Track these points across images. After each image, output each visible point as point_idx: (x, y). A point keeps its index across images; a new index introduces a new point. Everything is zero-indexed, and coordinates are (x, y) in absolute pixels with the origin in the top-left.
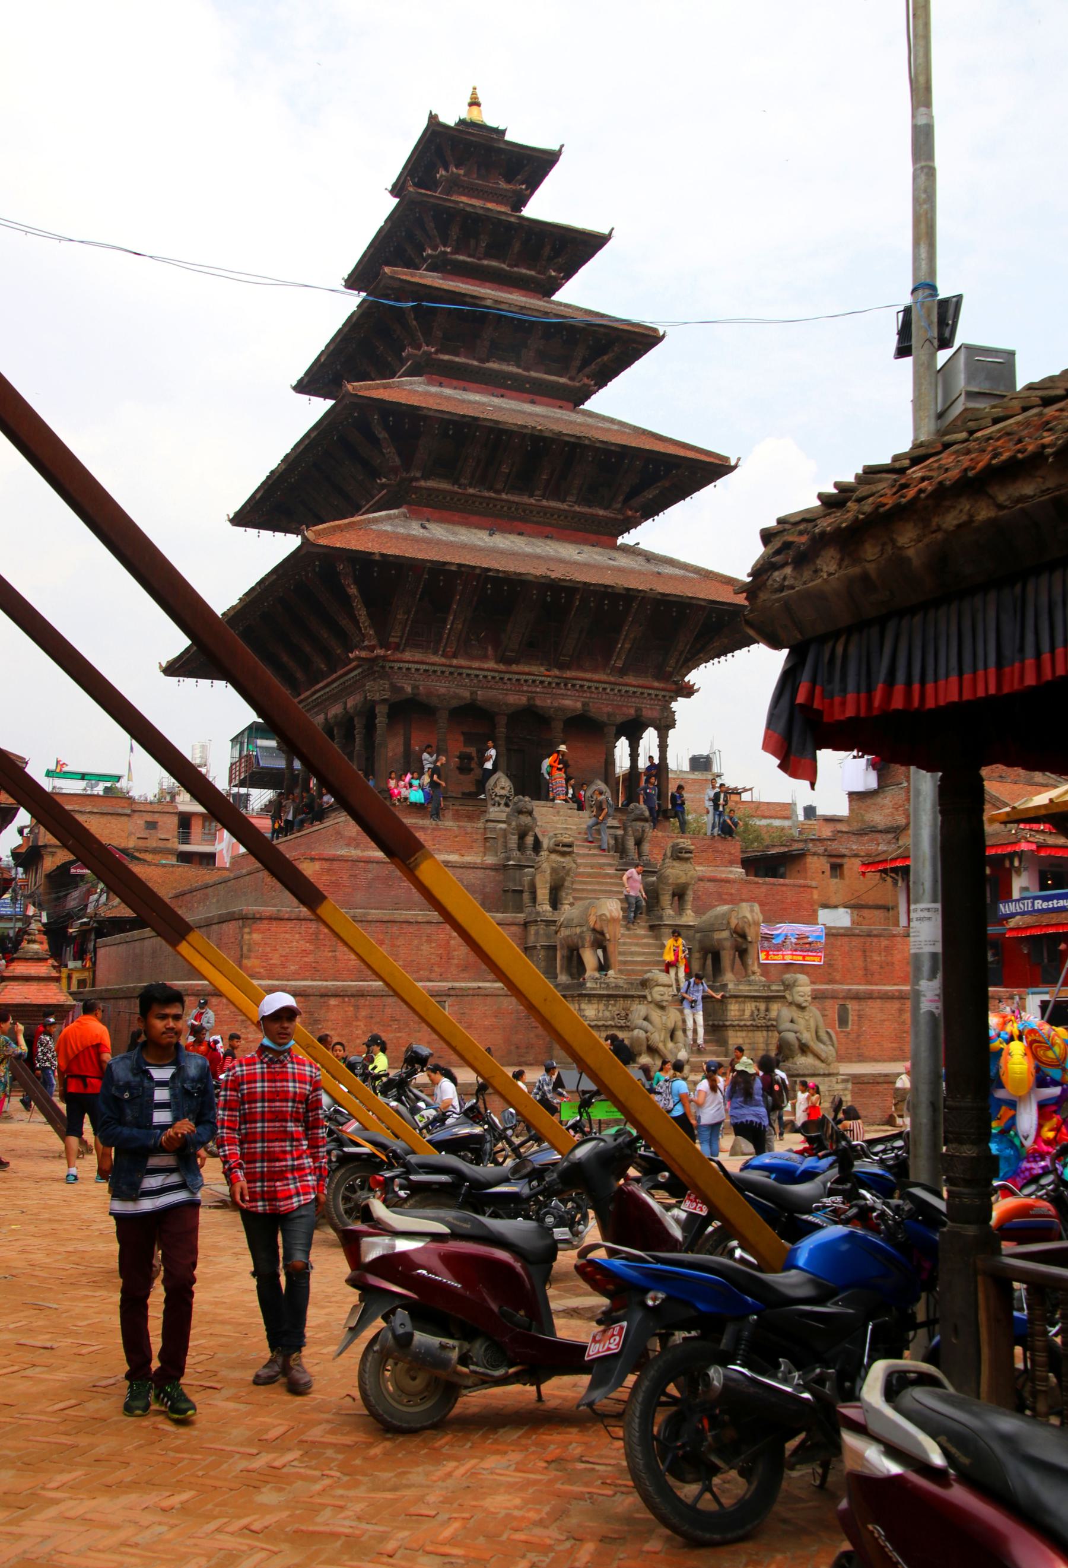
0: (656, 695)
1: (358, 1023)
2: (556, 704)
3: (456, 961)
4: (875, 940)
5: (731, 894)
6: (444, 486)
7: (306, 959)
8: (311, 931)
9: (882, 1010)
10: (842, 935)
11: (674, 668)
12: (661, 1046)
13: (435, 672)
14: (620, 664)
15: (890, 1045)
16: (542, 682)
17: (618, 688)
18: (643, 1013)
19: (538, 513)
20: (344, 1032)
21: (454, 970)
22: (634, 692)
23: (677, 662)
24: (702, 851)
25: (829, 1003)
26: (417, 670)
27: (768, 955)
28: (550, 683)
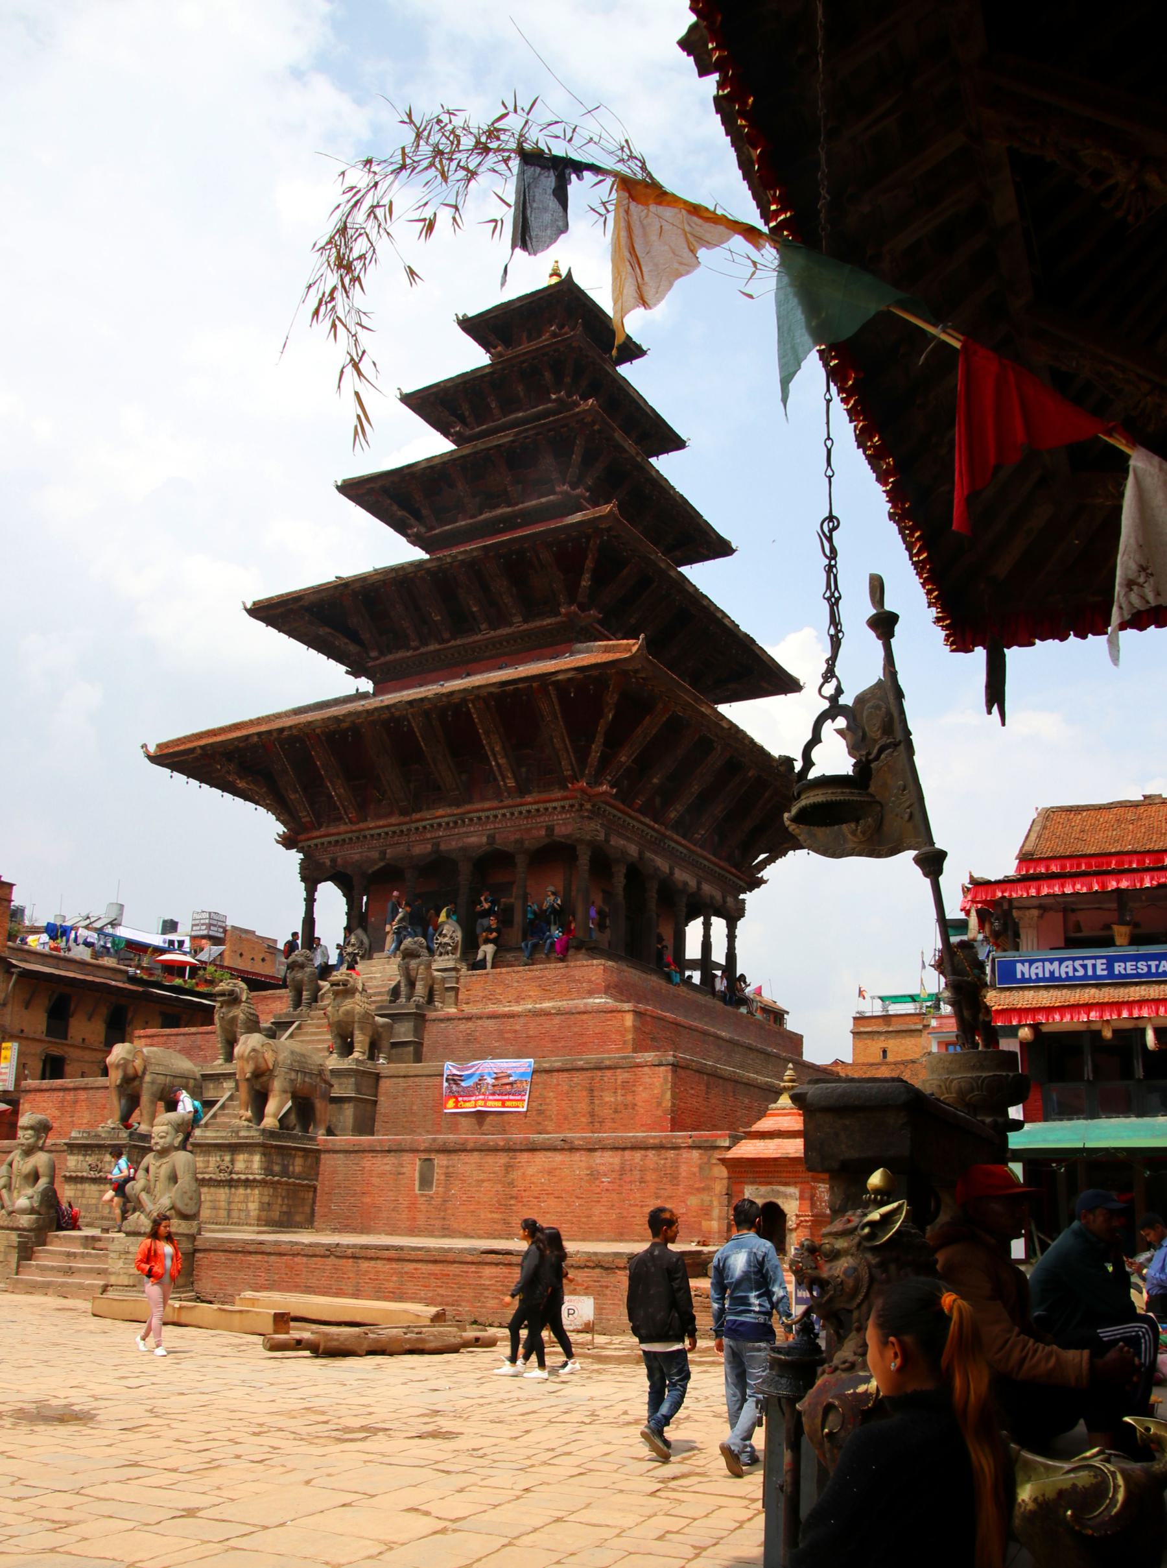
0: (563, 807)
2: (460, 845)
4: (608, 1073)
5: (516, 1031)
6: (401, 654)
9: (480, 1166)
10: (558, 1071)
11: (573, 769)
13: (344, 840)
14: (511, 783)
15: (489, 1216)
16: (440, 825)
17: (516, 811)
18: (10, 1158)
19: (487, 647)
22: (538, 810)
23: (572, 764)
24: (555, 983)
25: (407, 1157)
26: (330, 842)
27: (457, 1102)
28: (448, 824)
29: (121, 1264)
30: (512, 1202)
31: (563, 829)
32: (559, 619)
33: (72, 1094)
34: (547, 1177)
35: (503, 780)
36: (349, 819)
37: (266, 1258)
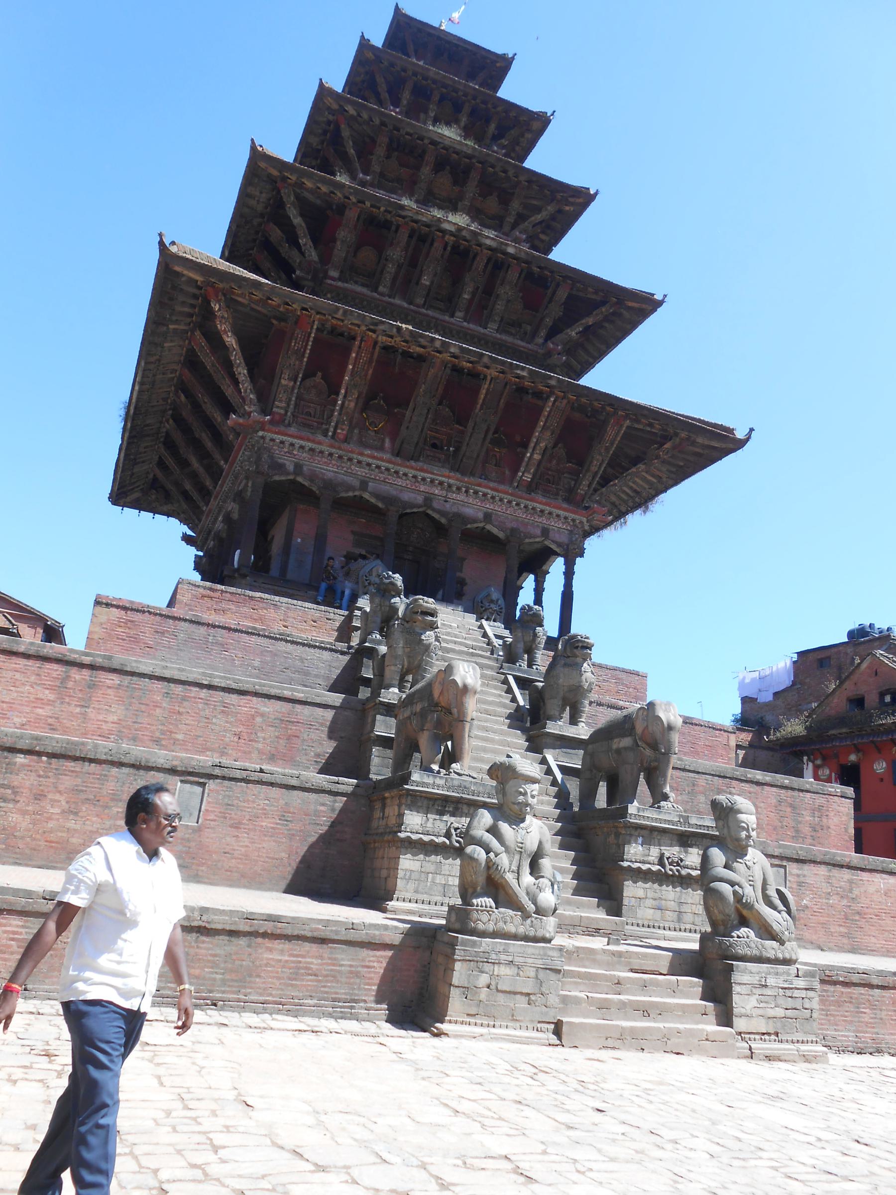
0: (566, 518)
1: (57, 797)
2: (455, 509)
3: (260, 746)
6: (365, 290)
7: (40, 711)
8: (55, 674)
12: (510, 877)
13: (321, 452)
14: (528, 477)
15: (838, 929)
16: (441, 483)
20: (30, 808)
21: (255, 755)
22: (542, 511)
23: (589, 486)
26: (302, 447)
29: (753, 1001)
30: (857, 918)
31: (557, 535)
32: (530, 346)
33: (86, 673)
34: (884, 897)
35: (523, 474)
36: (335, 432)
37: (871, 992)
